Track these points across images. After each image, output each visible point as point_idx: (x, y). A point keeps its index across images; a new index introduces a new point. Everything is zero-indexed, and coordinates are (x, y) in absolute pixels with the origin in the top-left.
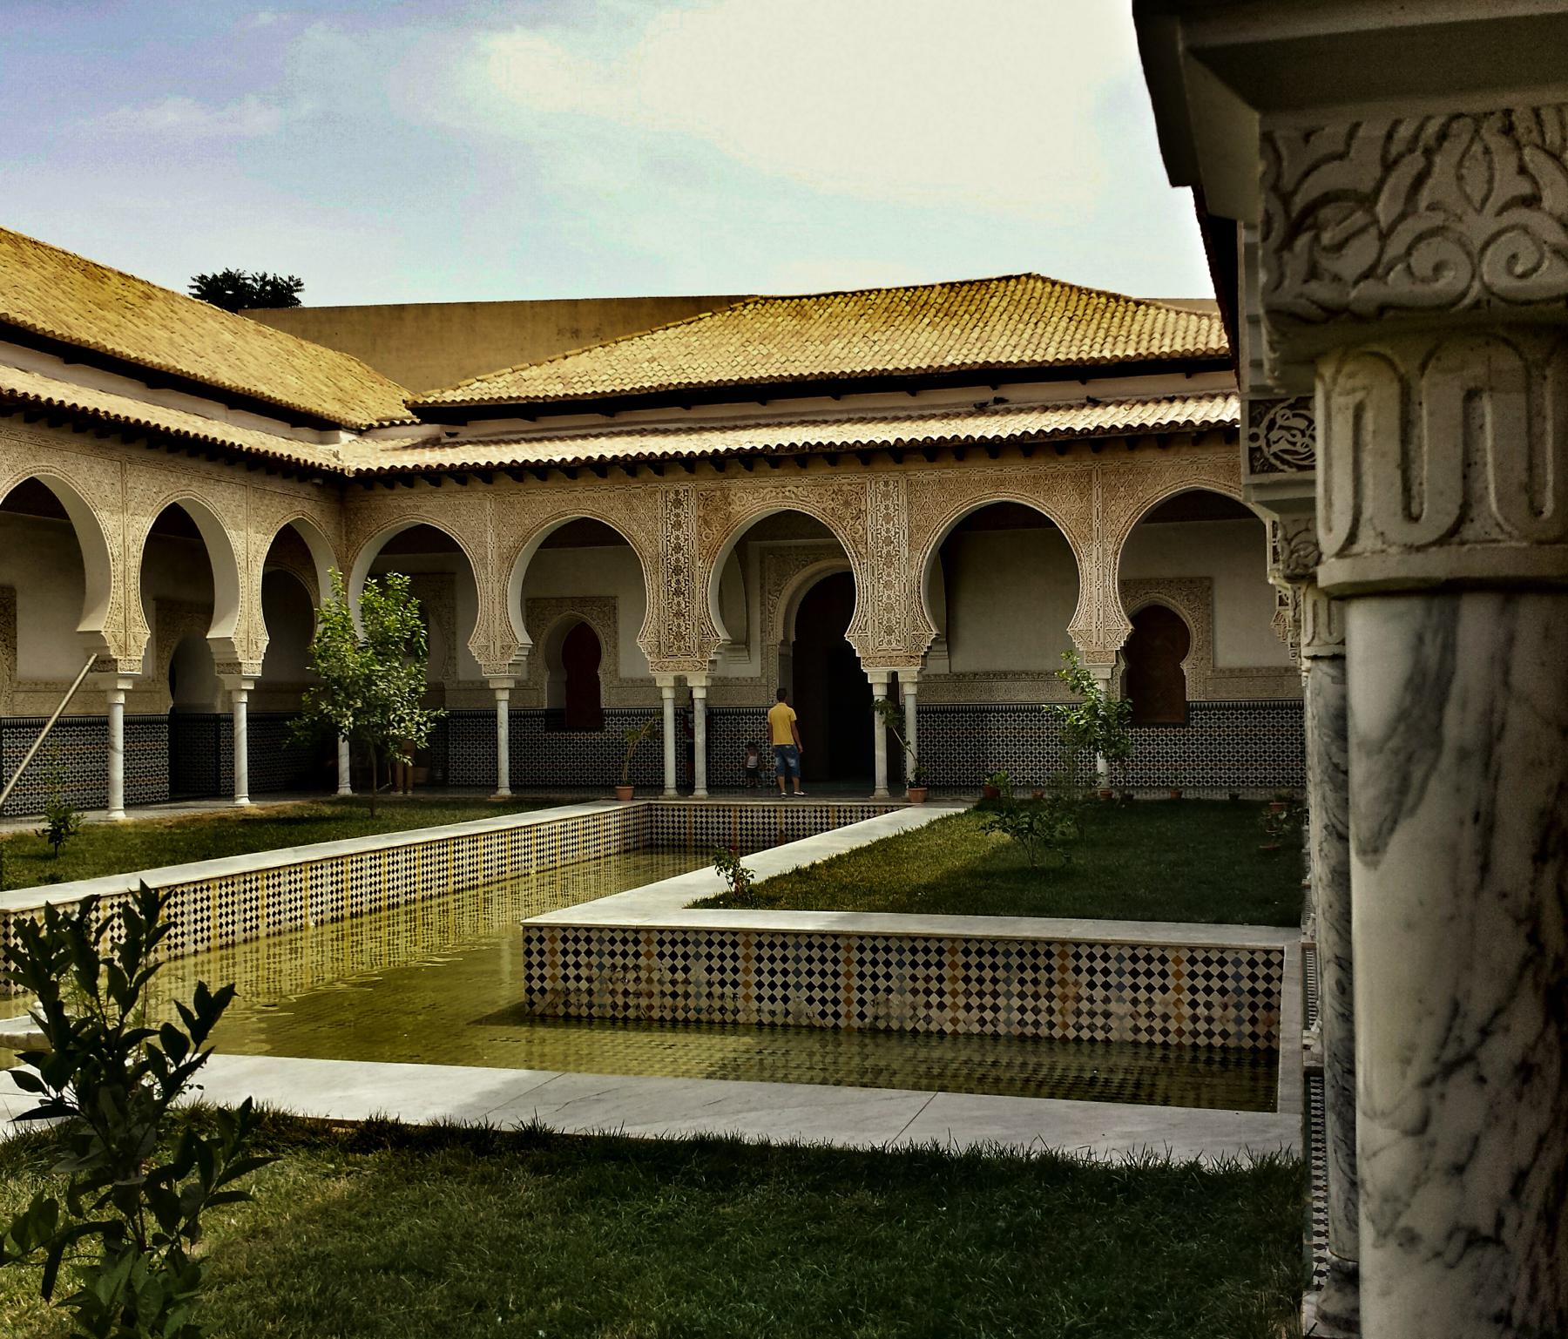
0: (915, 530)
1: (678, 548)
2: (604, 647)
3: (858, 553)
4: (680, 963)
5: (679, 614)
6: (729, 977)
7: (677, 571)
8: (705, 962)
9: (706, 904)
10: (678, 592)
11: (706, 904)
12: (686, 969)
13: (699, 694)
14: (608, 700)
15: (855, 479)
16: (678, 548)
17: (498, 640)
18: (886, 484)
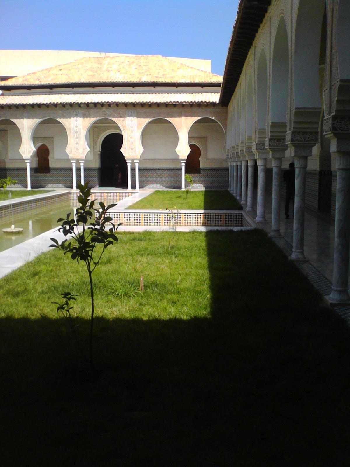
0: (139, 124)
1: (77, 127)
2: (50, 150)
3: (124, 129)
4: (128, 219)
5: (77, 144)
6: (138, 221)
7: (76, 132)
8: (134, 219)
9: (126, 209)
10: (77, 138)
11: (126, 209)
12: (130, 220)
13: (82, 164)
14: (51, 165)
15: (124, 110)
16: (77, 127)
17: (27, 150)
18: (131, 112)
